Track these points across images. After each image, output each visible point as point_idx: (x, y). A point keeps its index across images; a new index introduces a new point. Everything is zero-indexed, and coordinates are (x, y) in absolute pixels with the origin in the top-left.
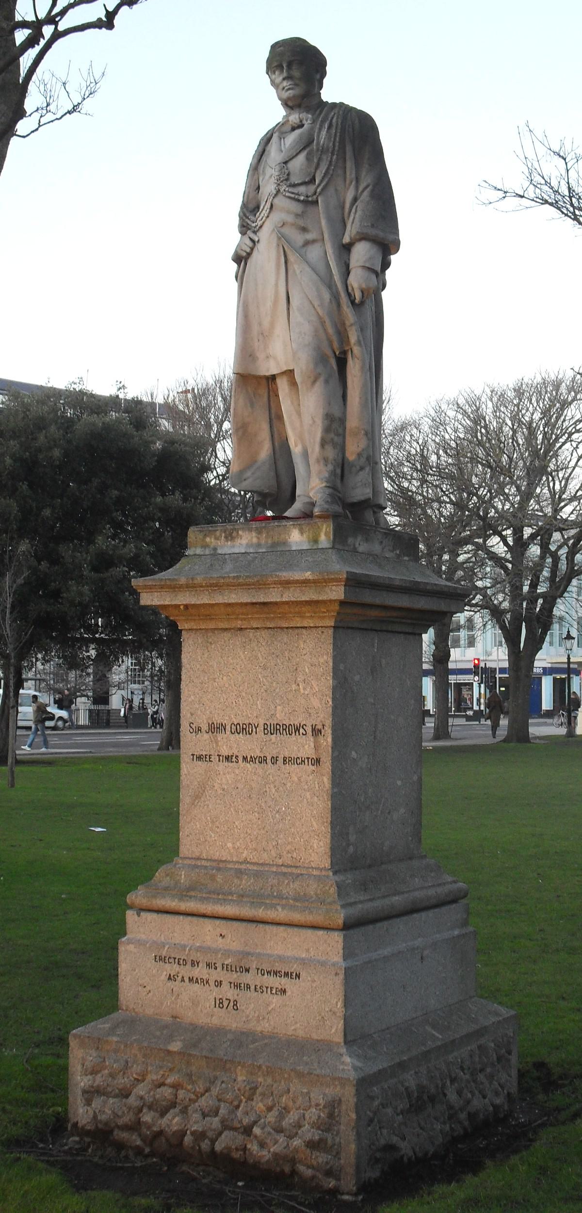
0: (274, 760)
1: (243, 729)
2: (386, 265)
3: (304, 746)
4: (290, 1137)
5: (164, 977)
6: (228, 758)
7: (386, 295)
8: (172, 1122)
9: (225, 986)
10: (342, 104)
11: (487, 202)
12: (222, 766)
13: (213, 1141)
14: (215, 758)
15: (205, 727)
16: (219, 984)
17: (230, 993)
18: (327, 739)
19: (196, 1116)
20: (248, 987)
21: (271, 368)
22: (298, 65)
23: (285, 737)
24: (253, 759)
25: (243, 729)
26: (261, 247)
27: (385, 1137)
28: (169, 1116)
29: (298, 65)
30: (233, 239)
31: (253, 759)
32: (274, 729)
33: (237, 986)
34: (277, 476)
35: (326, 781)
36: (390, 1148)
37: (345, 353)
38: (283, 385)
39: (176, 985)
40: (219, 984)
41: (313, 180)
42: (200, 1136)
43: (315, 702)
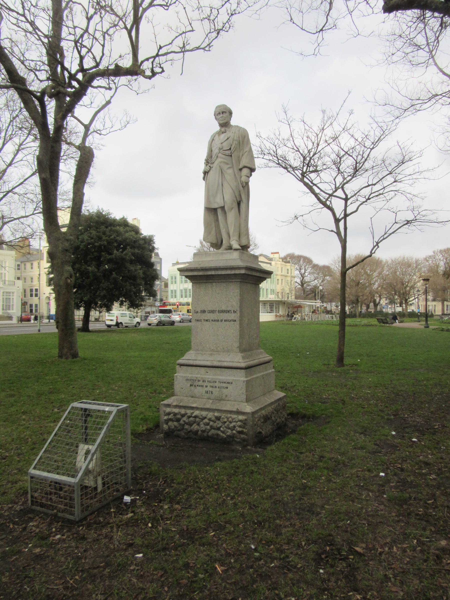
0: (222, 321)
1: (213, 312)
2: (251, 175)
3: (232, 316)
4: (232, 430)
5: (189, 385)
6: (207, 320)
7: (250, 184)
8: (195, 427)
9: (209, 387)
10: (238, 126)
11: (382, 102)
12: (205, 323)
13: (208, 432)
14: (203, 321)
15: (199, 312)
16: (207, 386)
17: (211, 389)
18: (238, 314)
19: (202, 426)
20: (216, 387)
21: (215, 206)
22: (224, 115)
23: (225, 314)
24: (215, 321)
25: (213, 312)
26: (213, 169)
27: (259, 430)
28: (193, 426)
29: (224, 115)
30: (202, 167)
31: (215, 321)
32: (223, 311)
33: (212, 387)
34: (217, 239)
35: (238, 326)
36: (260, 433)
37: (240, 201)
38: (219, 211)
39: (193, 388)
40: (207, 386)
41: (230, 149)
42: (203, 431)
43: (234, 303)
